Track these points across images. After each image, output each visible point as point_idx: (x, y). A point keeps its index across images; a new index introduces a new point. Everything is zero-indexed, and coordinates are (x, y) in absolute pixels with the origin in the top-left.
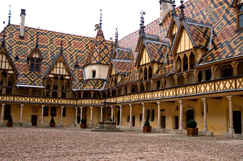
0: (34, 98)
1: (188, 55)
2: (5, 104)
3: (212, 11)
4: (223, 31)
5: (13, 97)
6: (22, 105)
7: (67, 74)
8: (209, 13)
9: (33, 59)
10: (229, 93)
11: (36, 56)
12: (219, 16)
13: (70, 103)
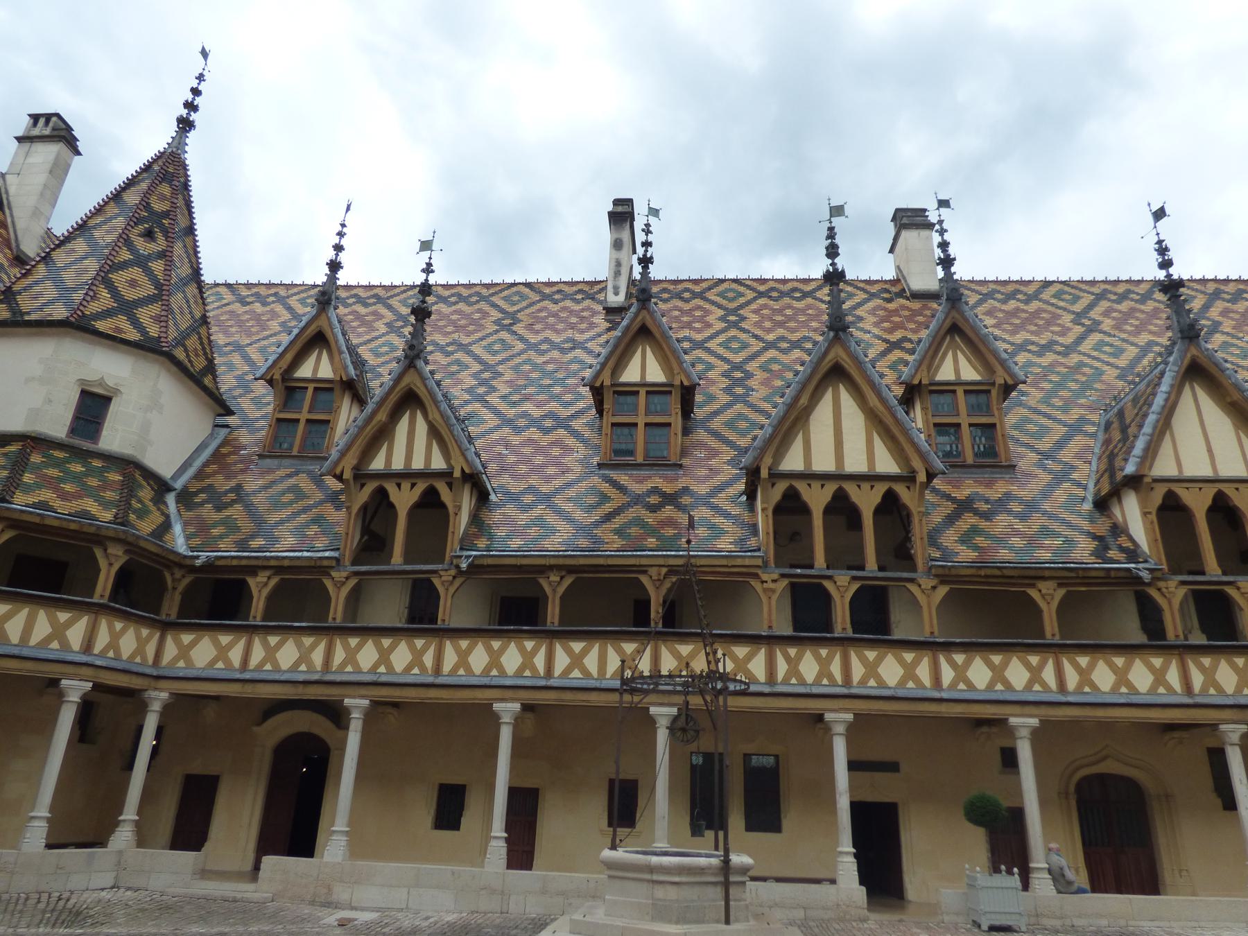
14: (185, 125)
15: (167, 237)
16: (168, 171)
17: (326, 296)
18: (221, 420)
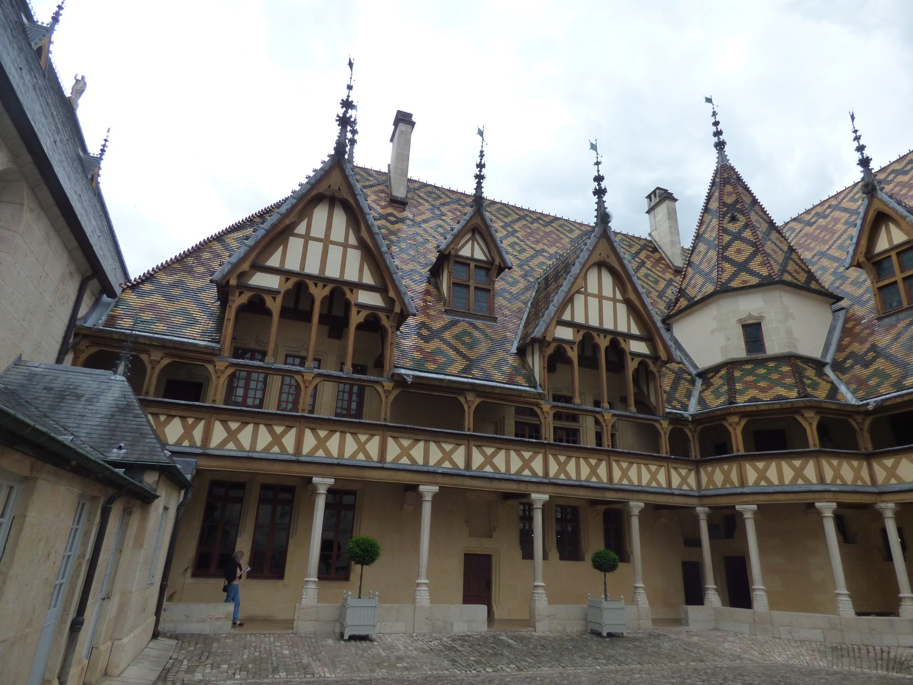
0: (489, 451)
2: (331, 481)
5: (376, 440)
6: (428, 490)
7: (635, 331)
9: (464, 262)
11: (473, 250)
13: (669, 482)
14: (720, 146)
15: (744, 214)
16: (726, 179)
17: (870, 186)
18: (835, 307)
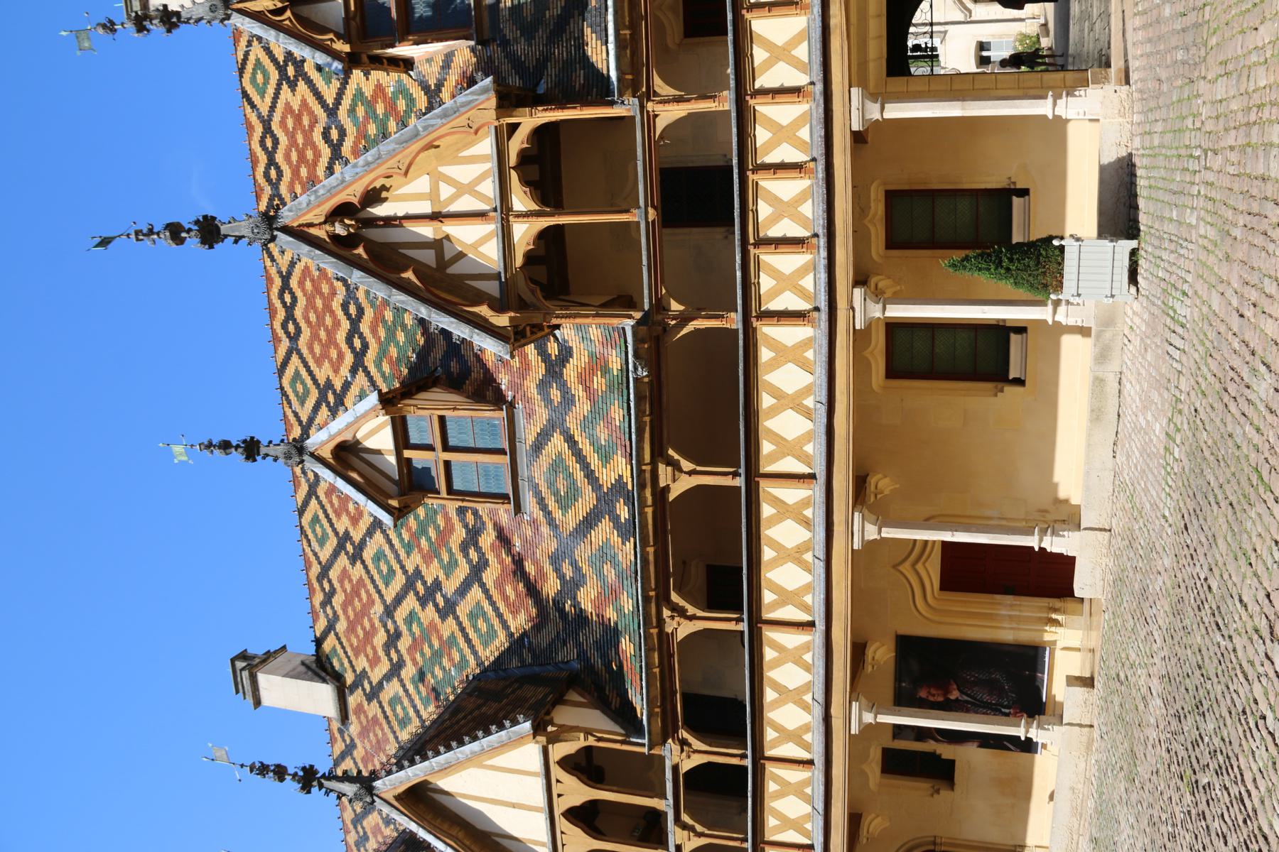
1: (576, 792)
3: (411, 688)
4: (505, 598)
8: (415, 707)
10: (839, 529)
12: (440, 638)
